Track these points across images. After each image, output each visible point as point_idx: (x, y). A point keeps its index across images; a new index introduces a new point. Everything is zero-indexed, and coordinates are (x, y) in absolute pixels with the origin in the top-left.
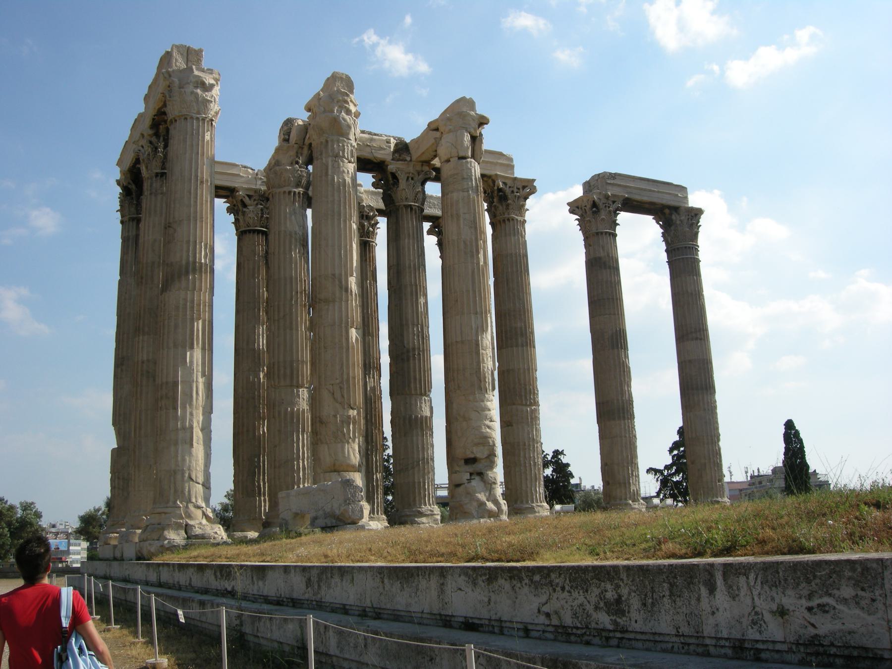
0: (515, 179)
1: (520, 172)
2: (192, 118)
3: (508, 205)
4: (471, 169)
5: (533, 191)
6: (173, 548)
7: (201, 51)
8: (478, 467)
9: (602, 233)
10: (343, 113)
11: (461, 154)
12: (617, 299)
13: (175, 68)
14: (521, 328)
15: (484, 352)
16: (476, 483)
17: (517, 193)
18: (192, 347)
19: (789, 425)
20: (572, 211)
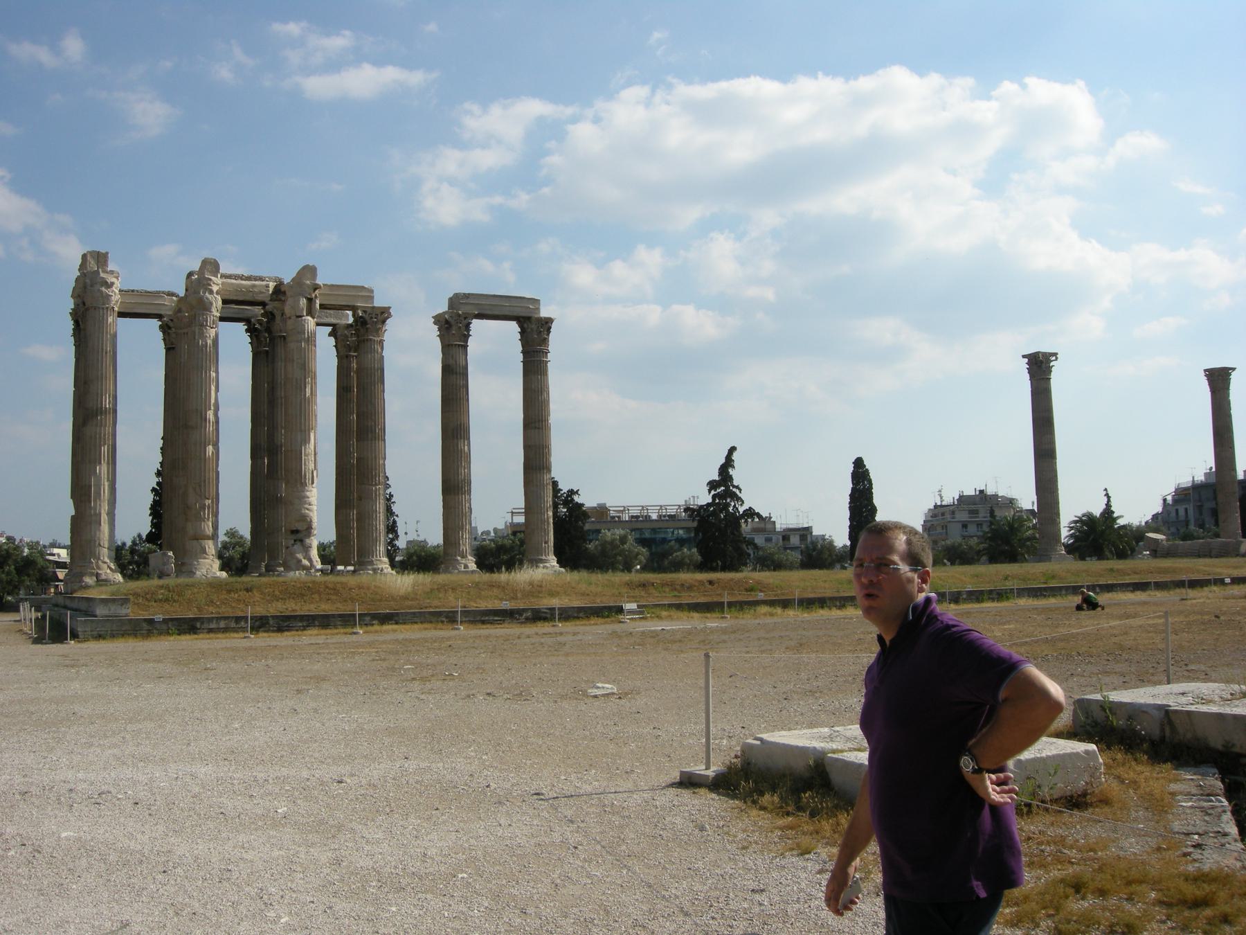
0: (374, 307)
1: (379, 302)
2: (99, 308)
3: (367, 329)
4: (304, 326)
5: (389, 316)
6: (87, 587)
7: (107, 253)
8: (299, 536)
9: (452, 345)
10: (207, 294)
11: (297, 314)
12: (460, 399)
13: (89, 269)
14: (371, 426)
15: (306, 458)
16: (297, 547)
17: (375, 318)
18: (100, 463)
19: (859, 463)
20: (435, 323)
